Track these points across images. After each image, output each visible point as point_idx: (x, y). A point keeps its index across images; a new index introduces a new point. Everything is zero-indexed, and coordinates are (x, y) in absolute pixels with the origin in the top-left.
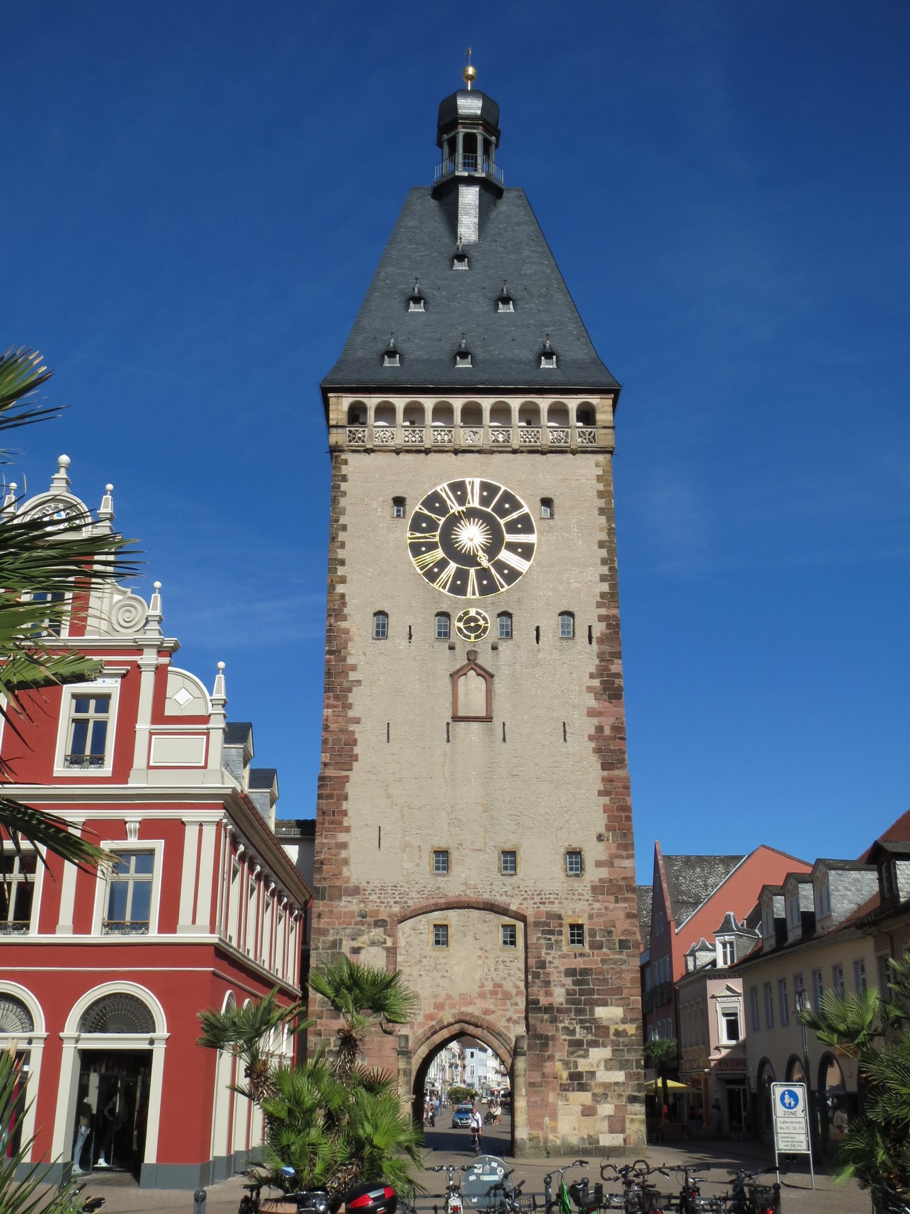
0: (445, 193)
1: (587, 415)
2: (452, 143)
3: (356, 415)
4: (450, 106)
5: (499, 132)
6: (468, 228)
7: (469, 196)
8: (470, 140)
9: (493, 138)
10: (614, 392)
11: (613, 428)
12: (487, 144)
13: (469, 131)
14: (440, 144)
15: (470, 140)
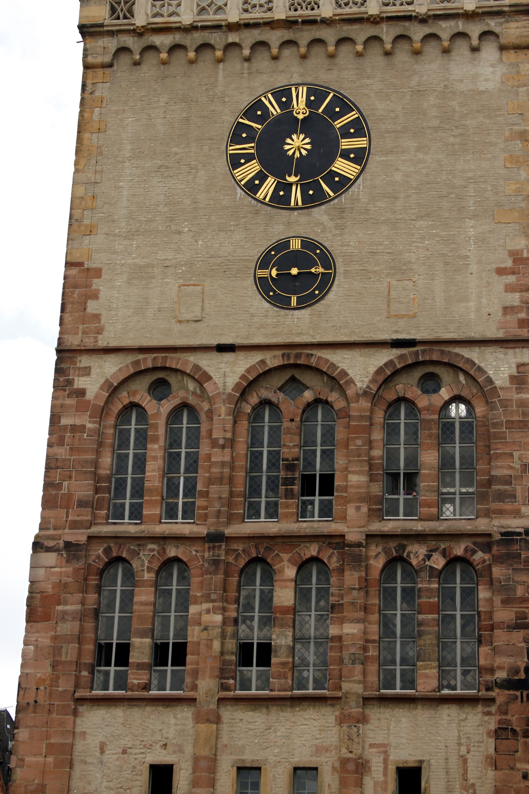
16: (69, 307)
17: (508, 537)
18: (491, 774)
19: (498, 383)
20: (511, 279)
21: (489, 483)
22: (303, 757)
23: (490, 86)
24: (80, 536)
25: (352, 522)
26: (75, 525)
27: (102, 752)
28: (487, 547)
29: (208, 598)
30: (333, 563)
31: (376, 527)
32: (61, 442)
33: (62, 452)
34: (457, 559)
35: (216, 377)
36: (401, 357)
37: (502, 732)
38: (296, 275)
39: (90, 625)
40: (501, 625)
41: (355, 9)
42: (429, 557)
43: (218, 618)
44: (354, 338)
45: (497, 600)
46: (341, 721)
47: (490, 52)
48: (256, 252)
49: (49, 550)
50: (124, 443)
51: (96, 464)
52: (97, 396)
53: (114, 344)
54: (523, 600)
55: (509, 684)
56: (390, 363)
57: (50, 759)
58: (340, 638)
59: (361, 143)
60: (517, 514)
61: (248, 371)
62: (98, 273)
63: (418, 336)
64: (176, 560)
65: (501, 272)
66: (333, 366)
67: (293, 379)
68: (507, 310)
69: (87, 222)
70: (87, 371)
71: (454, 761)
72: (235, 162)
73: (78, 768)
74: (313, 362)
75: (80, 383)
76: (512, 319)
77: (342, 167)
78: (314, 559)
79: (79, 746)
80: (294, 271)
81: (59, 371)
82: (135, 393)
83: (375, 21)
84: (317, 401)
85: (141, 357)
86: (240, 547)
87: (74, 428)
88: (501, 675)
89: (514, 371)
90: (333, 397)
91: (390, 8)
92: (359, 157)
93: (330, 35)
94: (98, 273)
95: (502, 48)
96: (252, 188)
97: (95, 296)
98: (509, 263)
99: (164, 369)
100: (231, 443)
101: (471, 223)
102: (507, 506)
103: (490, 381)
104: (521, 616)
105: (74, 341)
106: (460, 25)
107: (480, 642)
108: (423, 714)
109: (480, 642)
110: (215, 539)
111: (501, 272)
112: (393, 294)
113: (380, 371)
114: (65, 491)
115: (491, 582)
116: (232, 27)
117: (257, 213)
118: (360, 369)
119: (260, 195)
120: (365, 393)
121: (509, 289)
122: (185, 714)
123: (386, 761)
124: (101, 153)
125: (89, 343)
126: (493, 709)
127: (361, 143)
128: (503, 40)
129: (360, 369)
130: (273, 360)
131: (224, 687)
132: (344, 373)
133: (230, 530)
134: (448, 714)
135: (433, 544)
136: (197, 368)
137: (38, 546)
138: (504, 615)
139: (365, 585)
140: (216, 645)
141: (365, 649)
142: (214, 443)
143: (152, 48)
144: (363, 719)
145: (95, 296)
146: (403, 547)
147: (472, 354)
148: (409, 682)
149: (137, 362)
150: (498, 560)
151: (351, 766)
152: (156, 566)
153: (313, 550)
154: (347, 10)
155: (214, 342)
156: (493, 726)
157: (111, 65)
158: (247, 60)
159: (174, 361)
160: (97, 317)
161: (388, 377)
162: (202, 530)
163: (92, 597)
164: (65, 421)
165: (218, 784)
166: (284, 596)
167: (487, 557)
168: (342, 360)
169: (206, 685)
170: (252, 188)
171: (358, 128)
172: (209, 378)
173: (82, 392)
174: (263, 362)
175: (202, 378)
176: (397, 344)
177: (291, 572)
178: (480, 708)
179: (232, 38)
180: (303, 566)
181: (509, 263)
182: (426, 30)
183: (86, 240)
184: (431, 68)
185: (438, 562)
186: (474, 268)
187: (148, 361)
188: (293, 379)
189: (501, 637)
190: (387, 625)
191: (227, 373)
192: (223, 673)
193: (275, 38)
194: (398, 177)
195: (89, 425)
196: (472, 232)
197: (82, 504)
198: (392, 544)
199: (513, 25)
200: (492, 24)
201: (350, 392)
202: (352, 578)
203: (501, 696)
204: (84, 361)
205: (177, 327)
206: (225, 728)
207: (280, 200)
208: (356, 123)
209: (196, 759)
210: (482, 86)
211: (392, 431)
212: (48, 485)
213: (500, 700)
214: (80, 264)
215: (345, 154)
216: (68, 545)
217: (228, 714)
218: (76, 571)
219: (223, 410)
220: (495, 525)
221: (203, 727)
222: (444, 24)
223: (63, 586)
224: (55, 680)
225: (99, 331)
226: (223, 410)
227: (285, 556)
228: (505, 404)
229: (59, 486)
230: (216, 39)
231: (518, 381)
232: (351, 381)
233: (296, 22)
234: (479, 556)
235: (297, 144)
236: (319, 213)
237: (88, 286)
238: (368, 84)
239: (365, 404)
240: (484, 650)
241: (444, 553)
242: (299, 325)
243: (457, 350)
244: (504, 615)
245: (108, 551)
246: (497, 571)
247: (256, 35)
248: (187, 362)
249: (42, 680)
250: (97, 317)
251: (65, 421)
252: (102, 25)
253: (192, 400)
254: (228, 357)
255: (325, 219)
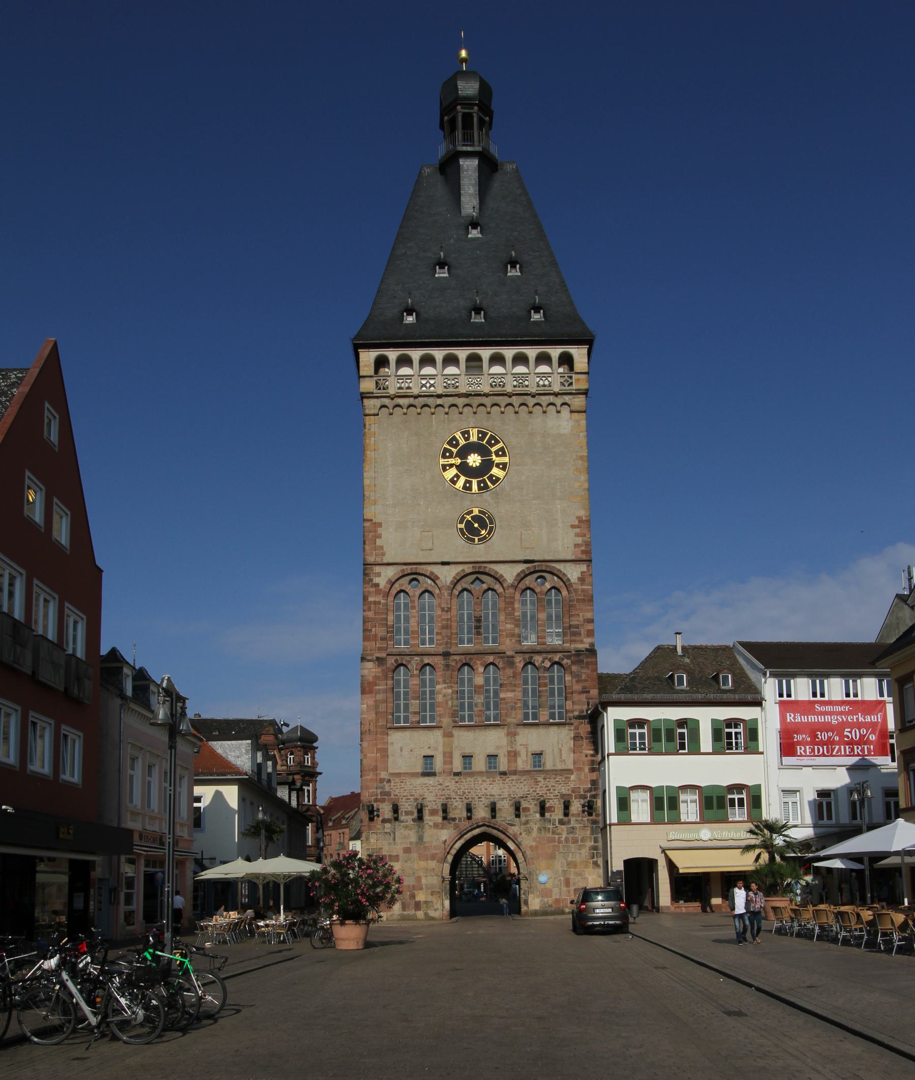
0: (448, 167)
1: (567, 360)
2: (453, 122)
3: (381, 362)
4: (451, 85)
5: (492, 112)
6: (469, 203)
7: (469, 167)
8: (467, 118)
9: (487, 119)
10: (587, 341)
11: (587, 373)
12: (481, 122)
13: (467, 111)
14: (442, 127)
15: (467, 118)
16: (367, 542)
17: (578, 652)
18: (572, 755)
19: (572, 581)
20: (578, 530)
21: (570, 627)
22: (492, 751)
23: (566, 431)
24: (384, 655)
25: (508, 645)
26: (380, 649)
27: (401, 750)
28: (568, 657)
29: (445, 682)
30: (501, 665)
31: (518, 648)
32: (369, 610)
33: (370, 614)
34: (556, 663)
35: (442, 577)
36: (528, 568)
37: (577, 738)
38: (476, 527)
39: (390, 695)
40: (576, 692)
41: (500, 389)
42: (543, 662)
43: (450, 691)
44: (505, 559)
45: (574, 680)
46: (508, 734)
47: (565, 411)
48: (457, 516)
49: (369, 661)
50: (398, 609)
51: (386, 619)
52: (385, 587)
53: (391, 561)
54: (585, 681)
55: (580, 717)
56: (523, 571)
57: (378, 755)
58: (504, 699)
59: (506, 460)
60: (582, 642)
61: (457, 574)
62: (380, 525)
63: (536, 558)
64: (428, 664)
65: (573, 527)
66: (496, 572)
67: (477, 578)
68: (576, 546)
69: (373, 498)
70: (379, 575)
71: (556, 750)
72: (444, 468)
73: (390, 759)
74: (487, 570)
75: (376, 580)
76: (578, 550)
77: (495, 471)
78: (492, 663)
79: (390, 749)
80: (476, 525)
81: (365, 574)
82: (402, 585)
83: (510, 395)
84: (489, 589)
85: (405, 567)
86: (457, 658)
87: (375, 603)
88: (576, 713)
89: (580, 575)
90: (497, 587)
91: (517, 389)
92: (503, 467)
93: (487, 401)
94: (380, 525)
95: (572, 412)
96: (453, 481)
97: (380, 537)
98: (577, 523)
99: (416, 574)
100: (449, 609)
101: (558, 502)
102: (578, 638)
103: (569, 580)
104: (584, 688)
105: (371, 559)
106: (552, 399)
107: (566, 699)
108: (542, 731)
109: (566, 699)
110: (446, 655)
111: (573, 527)
112: (523, 537)
113: (518, 575)
114: (373, 633)
115: (571, 673)
116: (439, 396)
117: (456, 495)
118: (509, 573)
119: (457, 486)
120: (512, 586)
121: (577, 535)
122: (438, 733)
123: (527, 751)
124: (376, 462)
125: (379, 560)
126: (572, 728)
127: (506, 460)
128: (573, 408)
129: (509, 573)
130: (468, 569)
131: (455, 722)
132: (502, 576)
133: (452, 651)
134: (554, 729)
135: (545, 655)
136: (432, 573)
137: (363, 659)
138: (577, 687)
139: (514, 676)
140: (450, 703)
141: (516, 703)
142: (443, 610)
143: (398, 406)
144: (515, 734)
145: (380, 537)
146: (532, 658)
147: (560, 566)
148: (535, 716)
149: (403, 570)
150: (573, 663)
151: (513, 754)
152: (419, 667)
153: (491, 659)
154: (496, 389)
155: (440, 561)
156: (572, 736)
157: (378, 415)
158: (447, 414)
159: (421, 569)
160: (381, 547)
161: (522, 577)
162: (441, 650)
163: (390, 682)
164: (371, 599)
165: (454, 764)
166: (479, 680)
167: (569, 661)
168: (500, 569)
169: (446, 721)
170: (453, 481)
171: (502, 452)
172: (438, 578)
173: (377, 585)
174: (463, 570)
175: (434, 578)
176: (526, 562)
177: (481, 669)
178: (567, 727)
179: (439, 401)
180: (486, 666)
181: (577, 523)
182: (534, 401)
183: (373, 508)
184: (537, 419)
185: (547, 664)
186: (560, 524)
187: (408, 569)
188: (477, 578)
189: (576, 697)
190: (525, 692)
191: (447, 575)
192: (454, 715)
193: (461, 401)
194: (523, 478)
195: (382, 601)
196: (559, 507)
197: (383, 639)
198: (527, 656)
199: (577, 400)
200: (567, 399)
201: (505, 585)
202: (509, 672)
203: (576, 722)
204: (377, 569)
205: (421, 553)
206: (455, 739)
207: (467, 487)
208: (502, 449)
209: (444, 753)
210: (563, 431)
211: (524, 603)
212: (364, 630)
213: (575, 724)
214: (371, 520)
215: (498, 465)
216: (378, 658)
217: (456, 732)
218: (383, 671)
219: (446, 593)
220: (574, 646)
221: (446, 739)
222: (543, 398)
223: (376, 677)
224: (377, 720)
225: (383, 554)
226: (446, 594)
227: (479, 662)
228: (576, 591)
229: (371, 631)
230: (430, 401)
231: (582, 580)
232: (505, 580)
233: (471, 395)
234: (565, 661)
235: (474, 460)
236: (486, 495)
237: (376, 531)
238: (506, 427)
239: (511, 590)
240: (569, 703)
241: (550, 660)
242: (479, 552)
243: (554, 565)
244: (577, 687)
245: (396, 661)
246: (574, 668)
247: (451, 400)
248: (426, 570)
249: (371, 721)
250: (381, 547)
251: (371, 599)
252: (372, 393)
253: (430, 589)
254: (447, 567)
255: (489, 498)
